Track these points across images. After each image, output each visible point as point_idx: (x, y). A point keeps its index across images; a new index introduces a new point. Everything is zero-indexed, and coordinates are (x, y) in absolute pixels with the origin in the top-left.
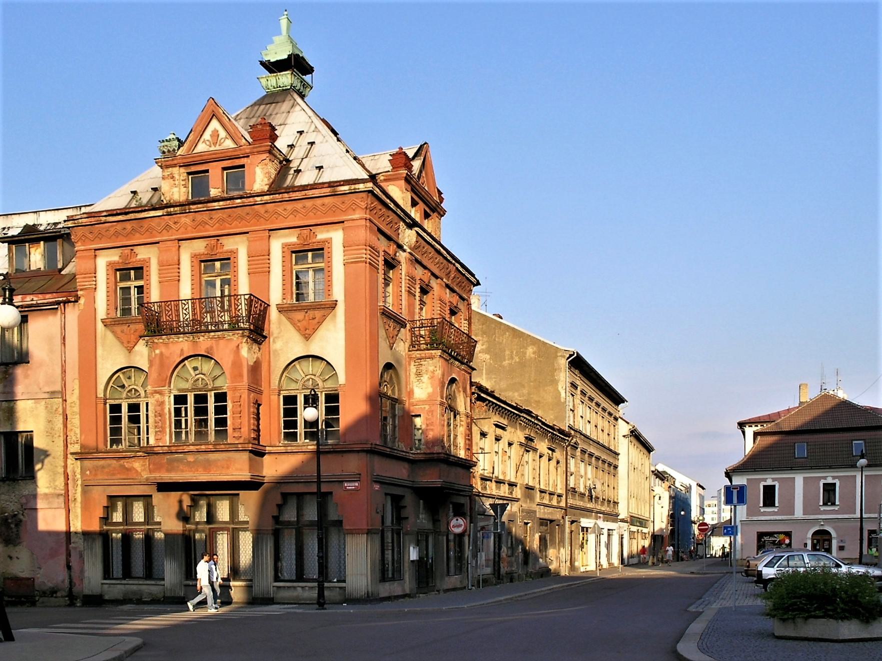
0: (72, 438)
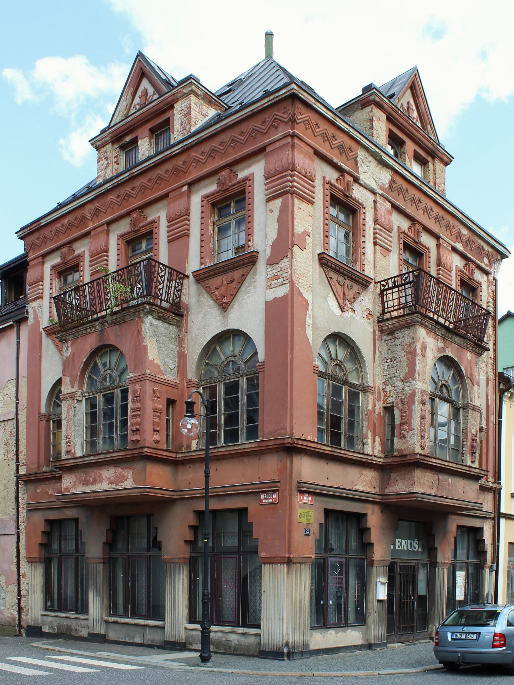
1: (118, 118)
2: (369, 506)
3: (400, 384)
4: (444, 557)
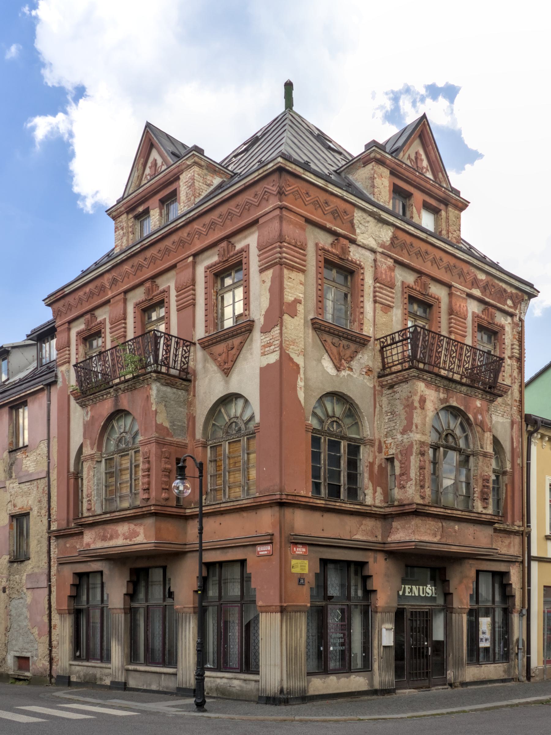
0: (53, 517)
1: (131, 189)
2: (370, 554)
3: (399, 437)
4: (461, 602)
